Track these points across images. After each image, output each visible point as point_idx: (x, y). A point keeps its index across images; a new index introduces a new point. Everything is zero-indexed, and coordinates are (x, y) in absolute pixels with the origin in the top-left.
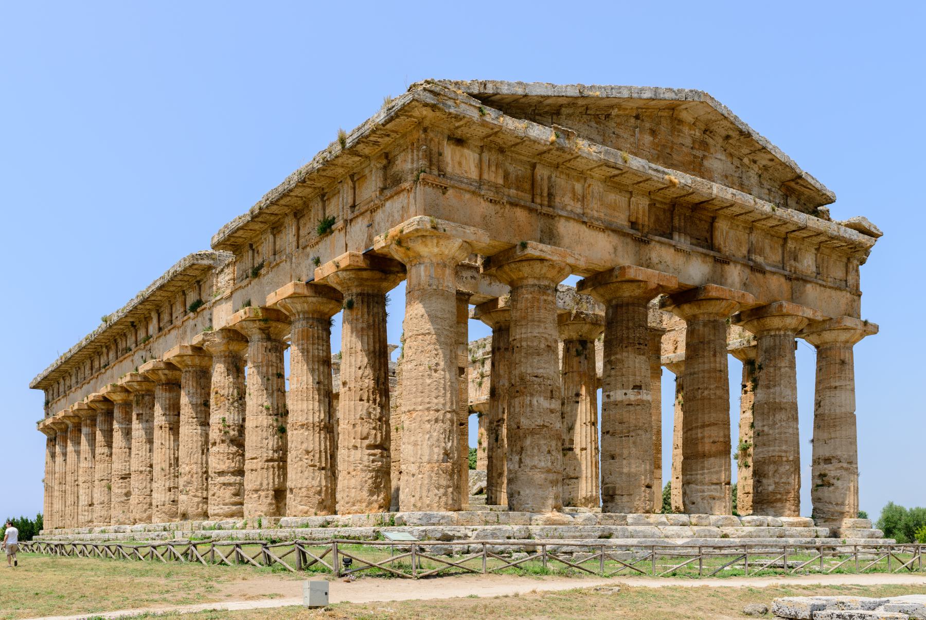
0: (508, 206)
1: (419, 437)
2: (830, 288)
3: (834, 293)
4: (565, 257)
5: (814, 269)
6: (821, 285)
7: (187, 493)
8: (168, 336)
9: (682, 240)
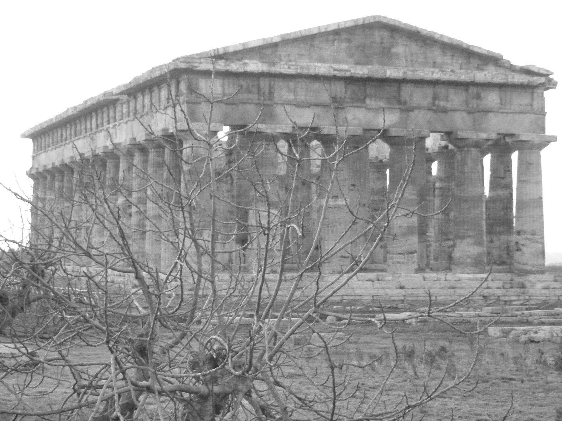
0: (240, 105)
2: (512, 113)
3: (517, 117)
4: (275, 129)
6: (503, 113)
9: (373, 103)
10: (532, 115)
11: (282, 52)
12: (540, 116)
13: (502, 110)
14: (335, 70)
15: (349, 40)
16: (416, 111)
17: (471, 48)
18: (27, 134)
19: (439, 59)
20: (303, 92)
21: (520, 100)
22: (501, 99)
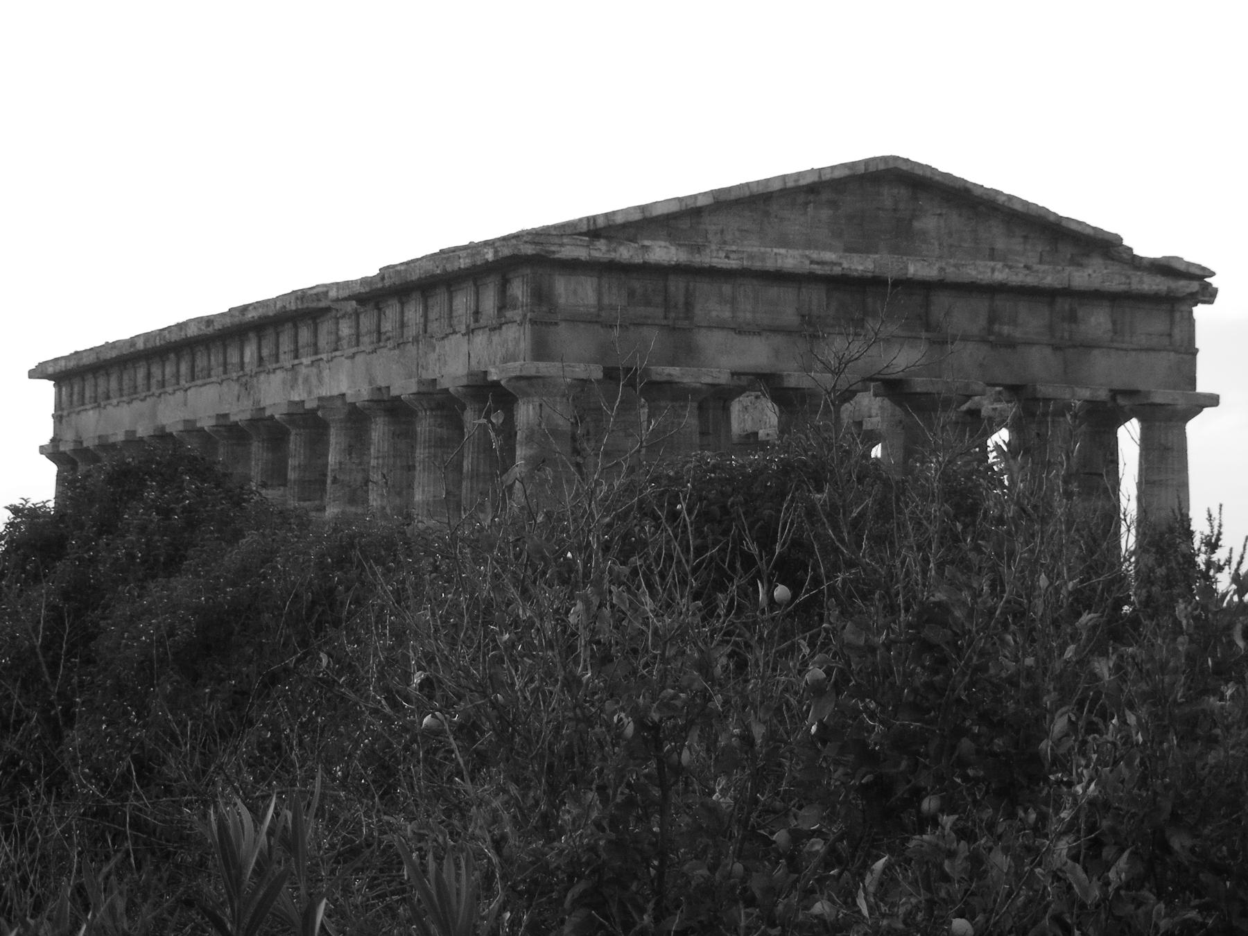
0: (632, 328)
2: (1134, 350)
3: (1143, 357)
5: (1110, 326)
6: (1117, 349)
10: (1172, 354)
11: (711, 225)
12: (1185, 356)
13: (1115, 345)
14: (812, 262)
15: (833, 204)
16: (958, 345)
17: (1064, 223)
18: (50, 370)
19: (1000, 244)
20: (750, 305)
21: (1151, 325)
22: (1114, 323)
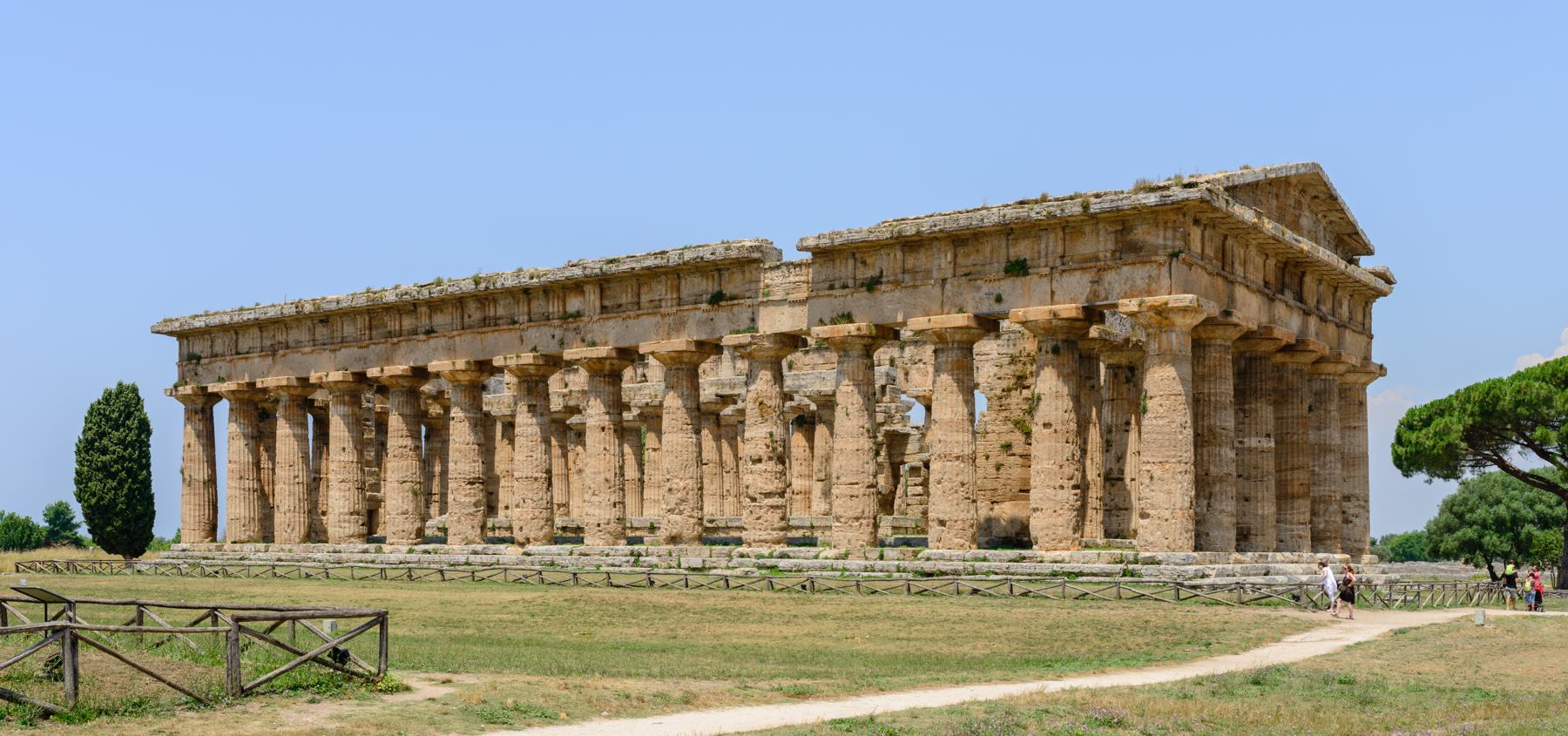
1: (1172, 487)
7: (681, 513)
8: (630, 322)
